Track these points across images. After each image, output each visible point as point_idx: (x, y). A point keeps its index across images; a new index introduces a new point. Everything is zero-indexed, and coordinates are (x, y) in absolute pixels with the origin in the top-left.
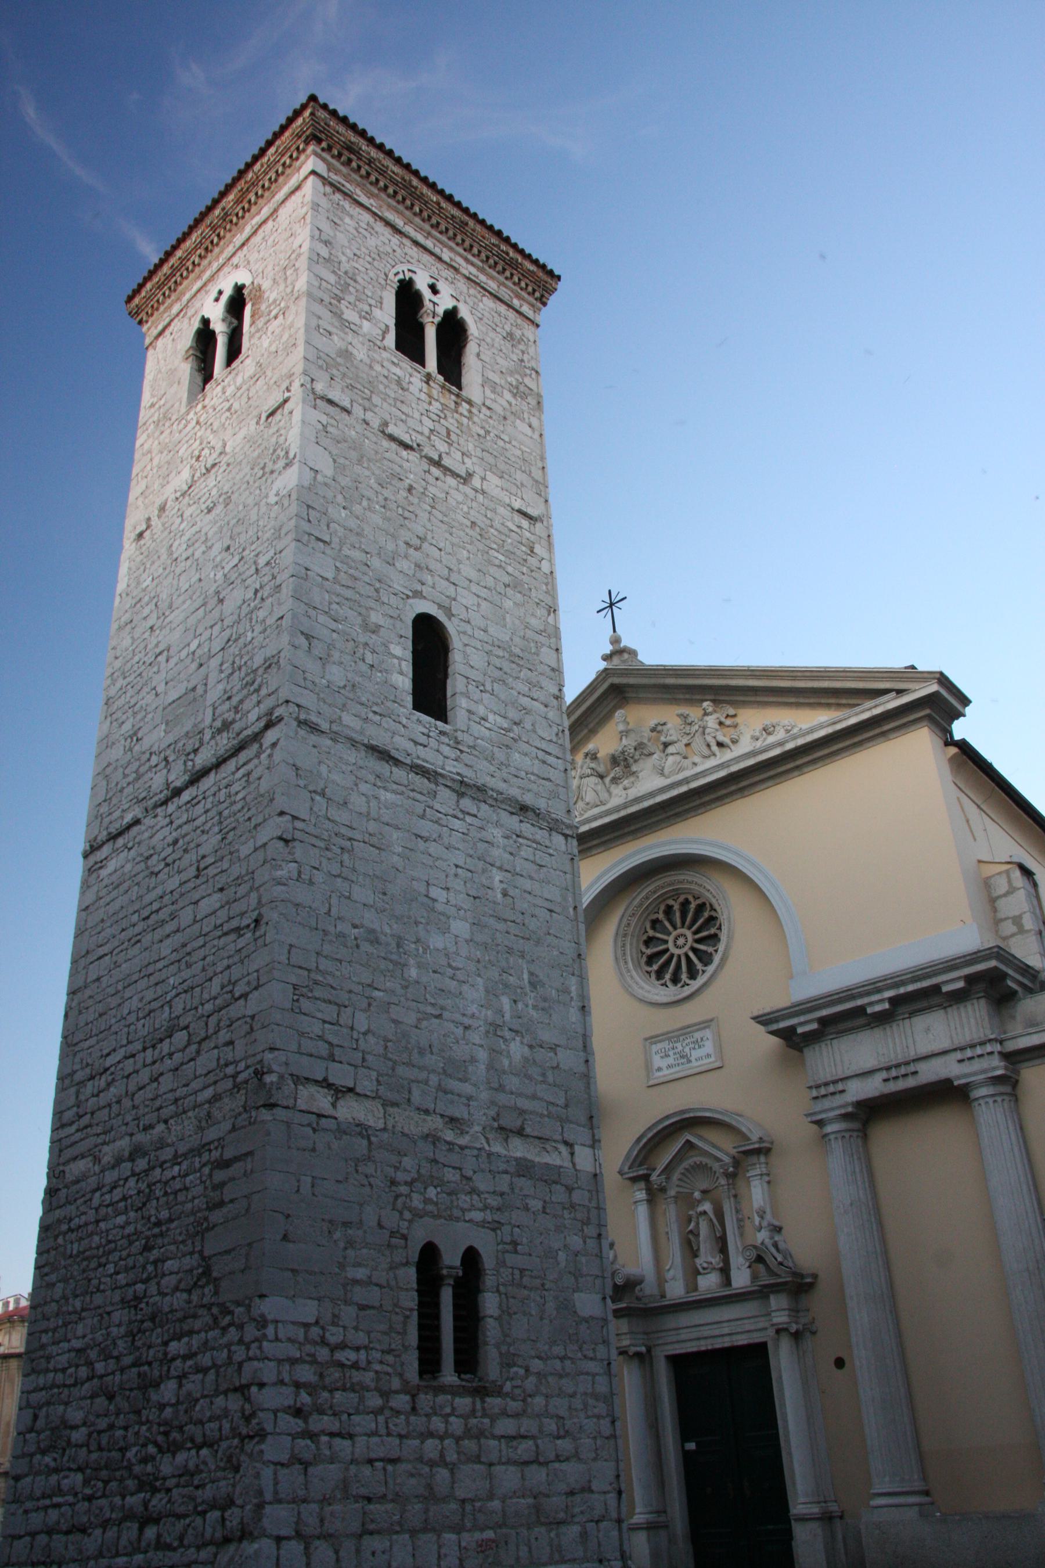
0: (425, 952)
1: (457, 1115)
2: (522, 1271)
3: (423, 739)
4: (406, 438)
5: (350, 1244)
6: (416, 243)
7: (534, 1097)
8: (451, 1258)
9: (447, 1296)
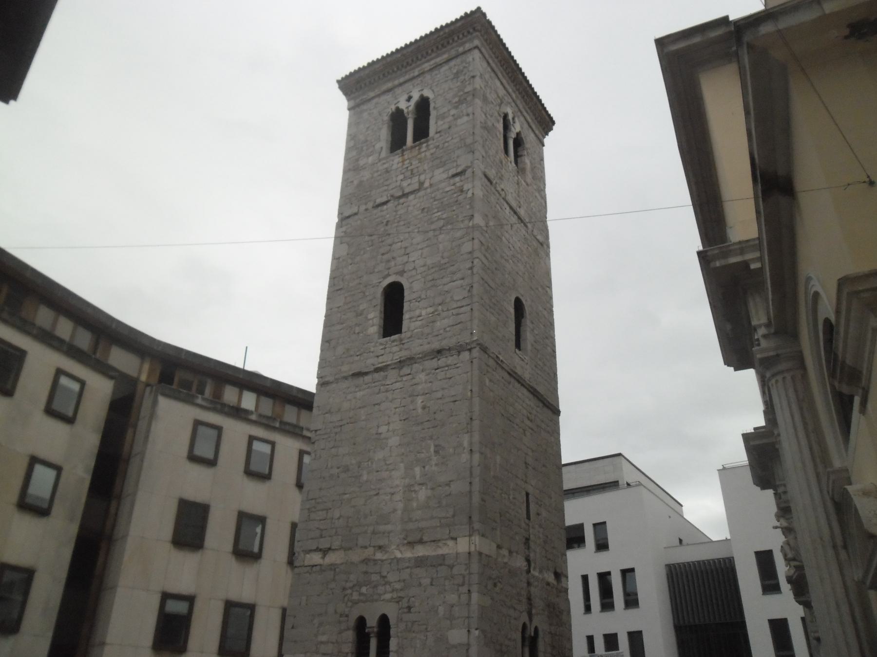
0: (372, 463)
1: (382, 544)
2: (414, 622)
3: (382, 352)
4: (384, 199)
5: (321, 624)
6: (401, 85)
7: (432, 518)
8: (372, 622)
9: (373, 643)
